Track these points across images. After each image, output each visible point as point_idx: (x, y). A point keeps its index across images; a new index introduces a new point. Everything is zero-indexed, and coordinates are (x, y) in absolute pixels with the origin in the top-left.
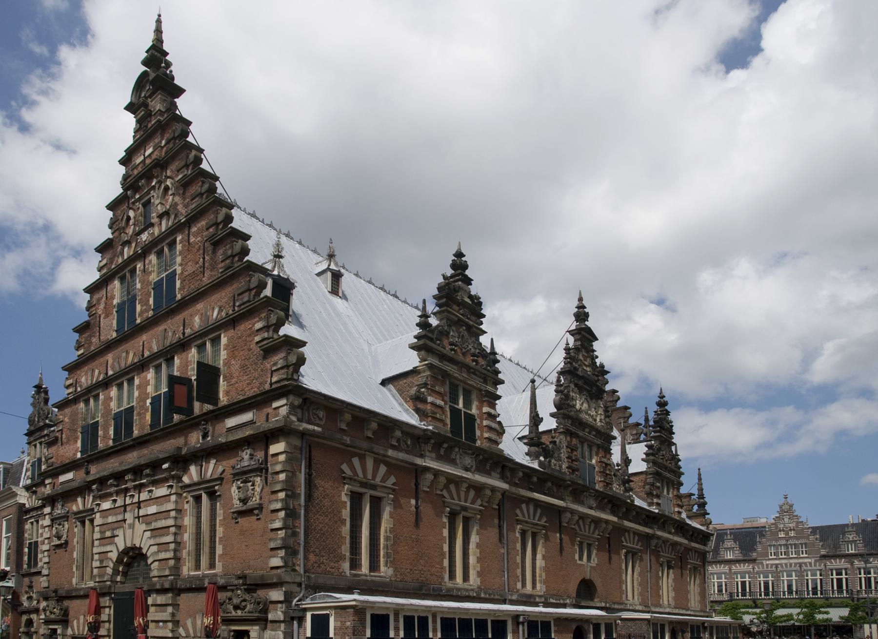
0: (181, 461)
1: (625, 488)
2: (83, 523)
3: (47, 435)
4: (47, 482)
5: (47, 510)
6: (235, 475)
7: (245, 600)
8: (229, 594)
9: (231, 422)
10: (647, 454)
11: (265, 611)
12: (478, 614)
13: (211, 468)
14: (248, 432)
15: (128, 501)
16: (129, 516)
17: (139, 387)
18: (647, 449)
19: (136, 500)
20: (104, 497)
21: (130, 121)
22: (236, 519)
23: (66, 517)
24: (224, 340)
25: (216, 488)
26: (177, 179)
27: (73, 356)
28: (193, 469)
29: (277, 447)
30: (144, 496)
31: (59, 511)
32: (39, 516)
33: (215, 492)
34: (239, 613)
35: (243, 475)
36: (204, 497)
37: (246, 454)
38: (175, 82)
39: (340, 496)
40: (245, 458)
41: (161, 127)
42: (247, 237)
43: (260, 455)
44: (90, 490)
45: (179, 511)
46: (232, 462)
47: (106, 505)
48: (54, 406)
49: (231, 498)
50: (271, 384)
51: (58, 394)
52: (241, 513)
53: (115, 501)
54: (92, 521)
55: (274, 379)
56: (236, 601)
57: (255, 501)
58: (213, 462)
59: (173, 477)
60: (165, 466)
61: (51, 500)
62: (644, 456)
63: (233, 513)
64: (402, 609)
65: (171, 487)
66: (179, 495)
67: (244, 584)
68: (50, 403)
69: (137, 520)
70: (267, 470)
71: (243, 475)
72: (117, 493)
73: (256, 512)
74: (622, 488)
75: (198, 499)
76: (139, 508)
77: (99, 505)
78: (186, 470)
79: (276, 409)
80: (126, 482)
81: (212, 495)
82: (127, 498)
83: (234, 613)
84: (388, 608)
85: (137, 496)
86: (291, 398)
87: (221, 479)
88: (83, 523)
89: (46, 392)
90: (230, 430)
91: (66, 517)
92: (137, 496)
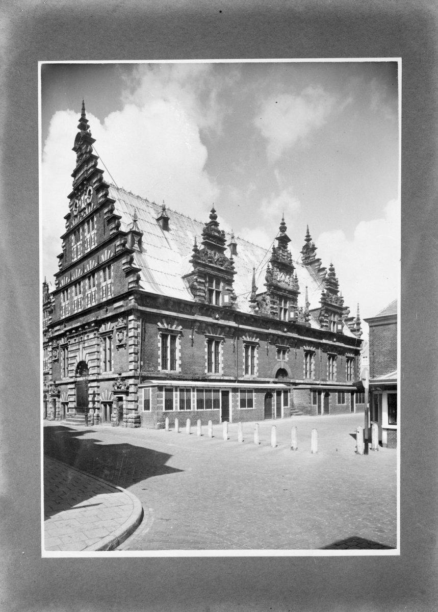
0: (99, 323)
1: (306, 319)
2: (64, 350)
3: (49, 308)
4: (50, 330)
5: (50, 344)
6: (117, 329)
7: (121, 384)
8: (115, 381)
9: (117, 305)
10: (322, 299)
11: (128, 388)
12: (214, 387)
13: (109, 326)
14: (123, 310)
16: (81, 346)
17: (83, 286)
18: (322, 296)
19: (83, 340)
20: (71, 338)
21: (74, 155)
23: (57, 347)
24: (112, 267)
26: (94, 187)
27: (57, 270)
28: (103, 326)
29: (131, 317)
31: (55, 345)
32: (47, 346)
33: (111, 336)
34: (119, 390)
35: (120, 330)
36: (107, 339)
37: (120, 320)
38: (92, 137)
39: (157, 337)
40: (120, 323)
41: (87, 161)
42: (120, 217)
44: (66, 336)
46: (116, 323)
47: (72, 341)
48: (52, 293)
49: (116, 340)
50: (129, 289)
51: (52, 289)
52: (120, 346)
53: (75, 340)
54: (67, 349)
55: (130, 286)
57: (123, 343)
58: (109, 323)
60: (93, 325)
61: (51, 339)
62: (320, 300)
64: (179, 386)
68: (50, 292)
71: (120, 330)
72: (77, 336)
74: (304, 320)
78: (100, 326)
79: (131, 300)
80: (79, 331)
81: (110, 338)
83: (117, 390)
84: (172, 386)
87: (112, 331)
88: (64, 350)
90: (115, 308)
91: (57, 347)
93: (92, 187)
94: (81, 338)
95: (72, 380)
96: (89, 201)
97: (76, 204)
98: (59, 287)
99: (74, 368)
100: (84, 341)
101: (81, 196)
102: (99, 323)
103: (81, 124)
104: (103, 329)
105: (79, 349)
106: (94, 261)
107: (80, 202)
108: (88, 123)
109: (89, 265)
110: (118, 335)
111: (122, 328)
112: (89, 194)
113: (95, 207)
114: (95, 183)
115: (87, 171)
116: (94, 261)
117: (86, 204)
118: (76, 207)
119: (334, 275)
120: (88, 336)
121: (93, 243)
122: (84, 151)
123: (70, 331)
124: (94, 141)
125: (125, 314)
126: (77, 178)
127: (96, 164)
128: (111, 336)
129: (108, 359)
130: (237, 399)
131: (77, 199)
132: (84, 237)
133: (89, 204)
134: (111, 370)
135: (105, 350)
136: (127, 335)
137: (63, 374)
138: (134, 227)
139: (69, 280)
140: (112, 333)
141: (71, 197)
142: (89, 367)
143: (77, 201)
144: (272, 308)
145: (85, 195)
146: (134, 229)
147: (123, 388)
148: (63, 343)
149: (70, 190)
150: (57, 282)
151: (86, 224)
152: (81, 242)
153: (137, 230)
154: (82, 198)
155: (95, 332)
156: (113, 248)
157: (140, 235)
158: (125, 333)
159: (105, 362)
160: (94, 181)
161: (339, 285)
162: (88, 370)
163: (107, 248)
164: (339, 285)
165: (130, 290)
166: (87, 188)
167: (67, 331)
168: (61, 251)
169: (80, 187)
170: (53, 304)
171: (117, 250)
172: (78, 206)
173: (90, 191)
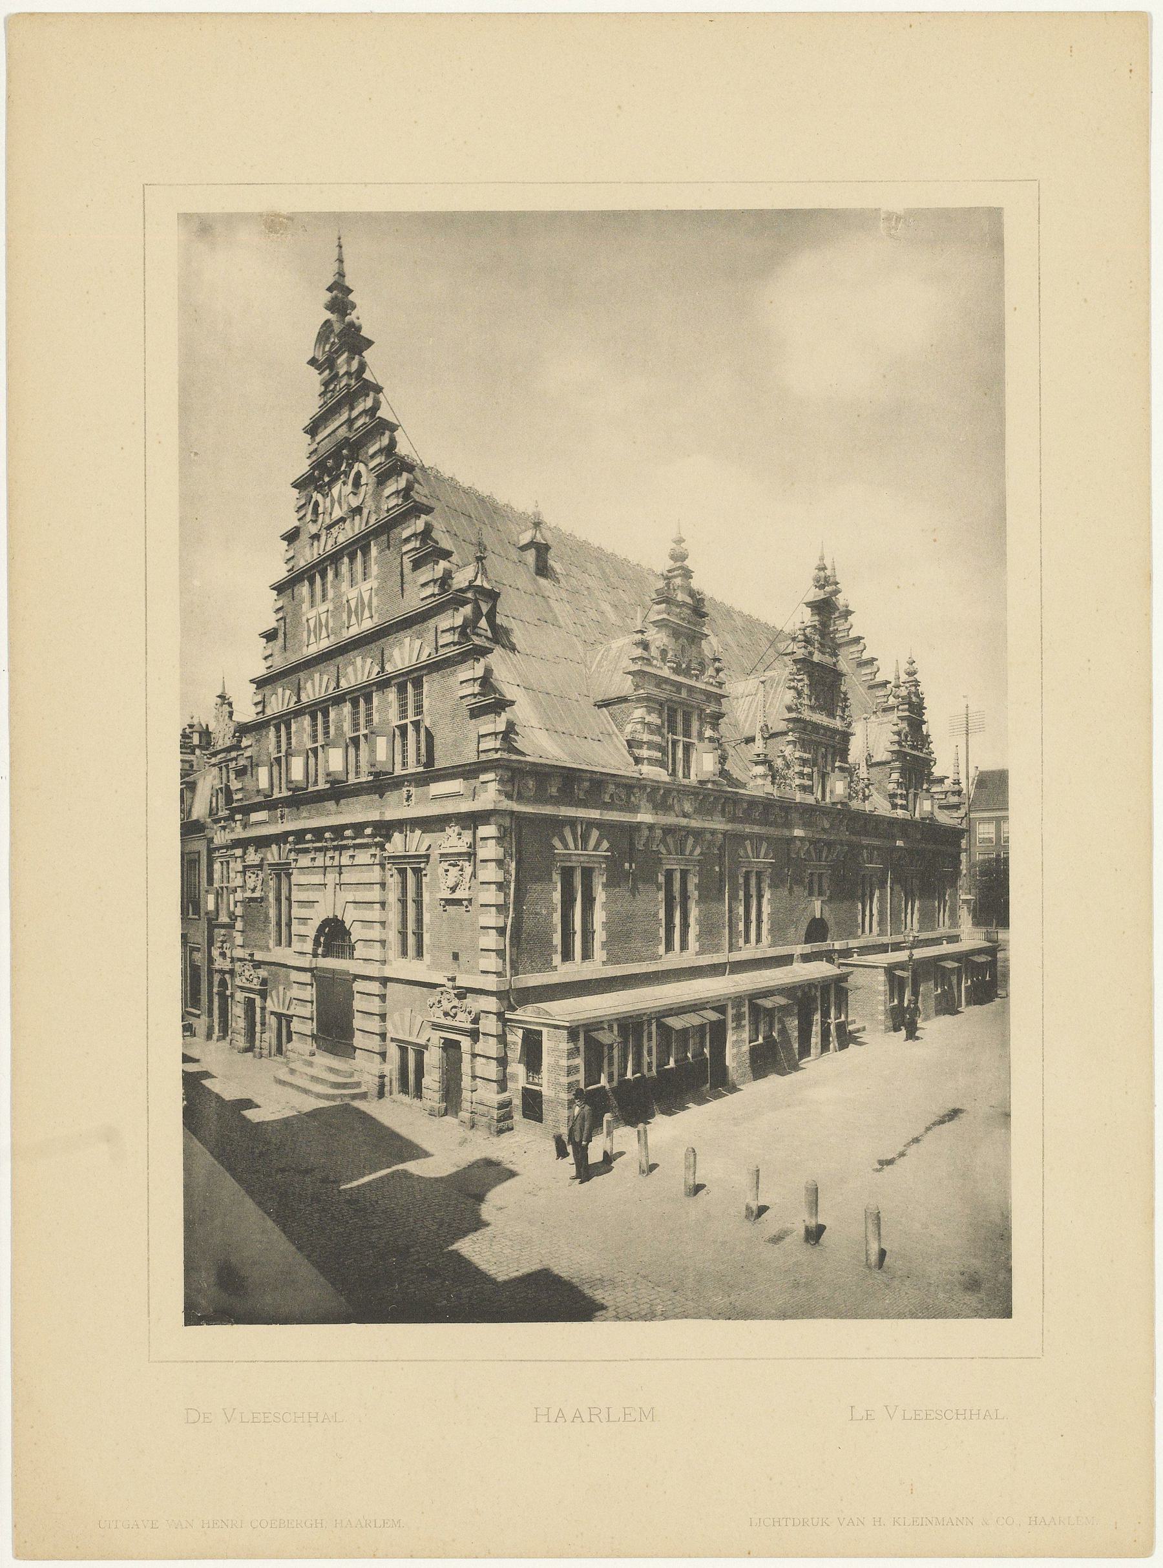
15: (328, 863)
19: (336, 863)
22: (444, 907)
25: (422, 865)
29: (488, 830)
30: (345, 860)
33: (421, 870)
43: (467, 836)
45: (383, 885)
47: (305, 861)
53: (313, 859)
56: (447, 1006)
59: (376, 845)
63: (442, 899)
65: (374, 856)
66: (382, 866)
67: (454, 988)
69: (338, 887)
70: (475, 854)
72: (317, 850)
73: (465, 903)
75: (402, 872)
76: (340, 874)
77: (296, 860)
81: (417, 872)
82: (327, 859)
85: (337, 858)
86: (500, 772)
89: (230, 704)
92: (337, 858)
93: (366, 465)
94: (332, 858)
95: (305, 962)
96: (355, 502)
97: (317, 504)
98: (263, 712)
99: (311, 930)
100: (340, 867)
101: (330, 485)
102: (385, 829)
103: (335, 299)
104: (397, 844)
105: (325, 885)
106: (369, 660)
107: (328, 499)
108: (351, 297)
109: (355, 670)
110: (447, 871)
111: (460, 854)
112: (357, 484)
113: (372, 521)
114: (373, 457)
115: (350, 422)
116: (369, 660)
117: (345, 507)
118: (315, 511)
119: (916, 684)
120: (353, 857)
121: (367, 614)
122: (342, 372)
123: (300, 835)
124: (369, 343)
125: (472, 820)
126: (318, 438)
127: (376, 407)
128: (421, 870)
129: (411, 926)
130: (734, 1011)
131: (319, 489)
132: (338, 596)
133: (358, 510)
134: (420, 953)
135: (403, 902)
136: (474, 875)
137: (273, 935)
138: (479, 575)
139: (295, 699)
140: (427, 862)
141: (300, 485)
142: (347, 925)
143: (317, 496)
144: (801, 774)
145: (344, 483)
146: (478, 582)
147: (461, 1016)
148: (277, 861)
149: (302, 467)
150: (259, 698)
151: (346, 560)
152: (329, 605)
153: (486, 585)
154: (335, 491)
155: (373, 851)
156: (431, 636)
157: (493, 596)
158: (469, 870)
159: (403, 934)
160: (371, 451)
161: (925, 708)
162: (353, 948)
163: (409, 632)
164: (925, 708)
165: (483, 757)
166: (351, 466)
167: (287, 834)
168: (270, 623)
169: (330, 463)
170: (247, 754)
171: (441, 642)
172: (321, 510)
173: (358, 475)
